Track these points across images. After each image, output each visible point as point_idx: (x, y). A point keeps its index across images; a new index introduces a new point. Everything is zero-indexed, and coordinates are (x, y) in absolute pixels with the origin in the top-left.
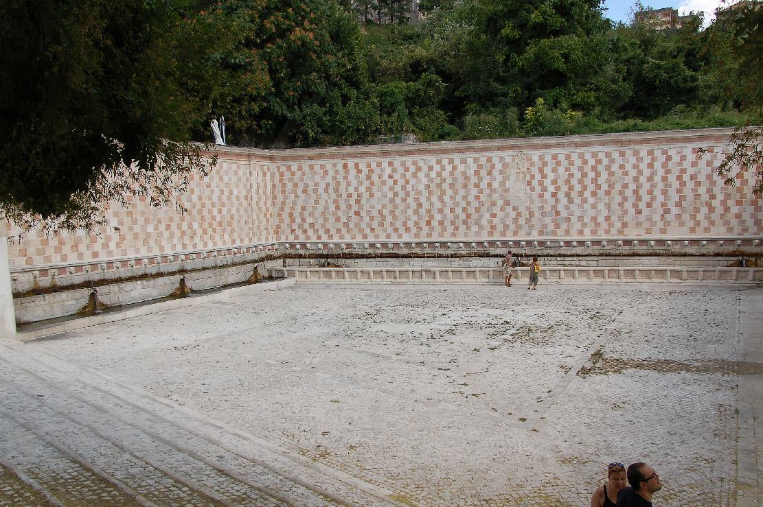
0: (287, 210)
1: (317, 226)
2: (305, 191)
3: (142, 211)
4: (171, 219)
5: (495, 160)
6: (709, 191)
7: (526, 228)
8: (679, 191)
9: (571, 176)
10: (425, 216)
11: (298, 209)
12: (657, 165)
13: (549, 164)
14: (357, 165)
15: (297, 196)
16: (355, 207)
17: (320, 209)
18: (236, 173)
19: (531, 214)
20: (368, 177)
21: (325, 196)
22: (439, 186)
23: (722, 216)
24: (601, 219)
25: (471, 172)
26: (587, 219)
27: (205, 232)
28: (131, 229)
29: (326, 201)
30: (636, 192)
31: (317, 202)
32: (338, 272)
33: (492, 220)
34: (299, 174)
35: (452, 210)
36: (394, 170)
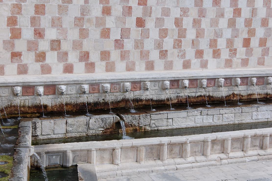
1: (65, 46)
32: (171, 145)
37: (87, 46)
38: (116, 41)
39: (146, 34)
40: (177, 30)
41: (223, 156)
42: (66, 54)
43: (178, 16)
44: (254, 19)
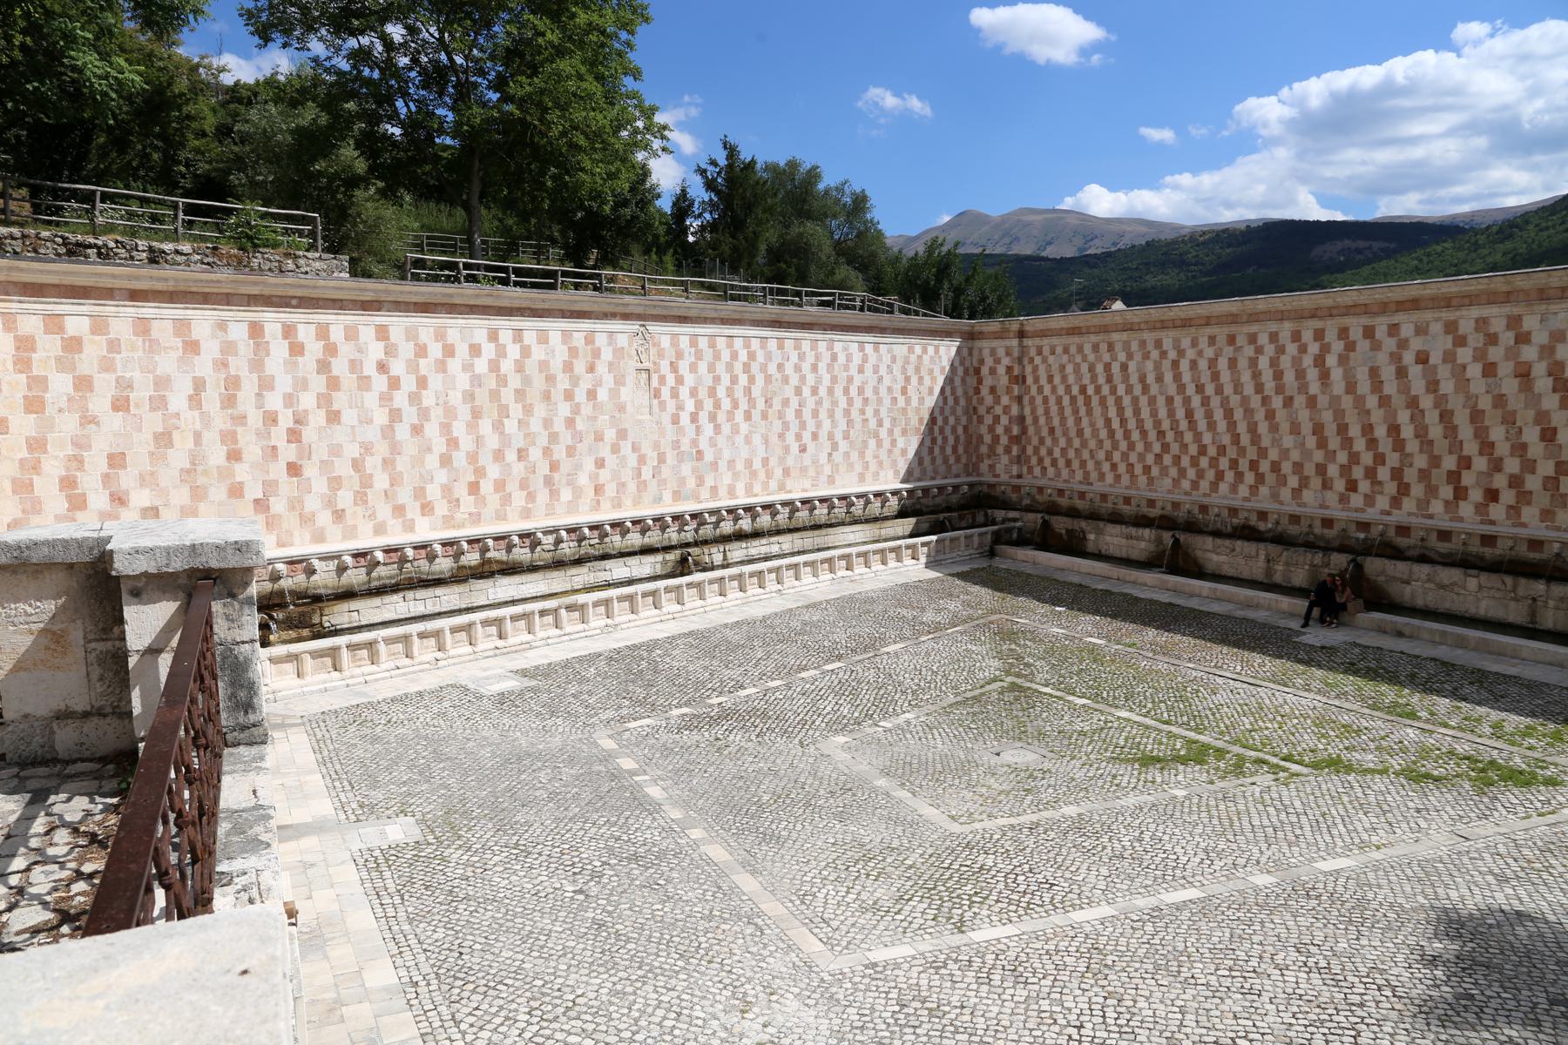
0: (53, 467)
2: (120, 405)
5: (601, 340)
6: (877, 412)
7: (653, 486)
8: (847, 412)
9: (717, 379)
12: (822, 366)
13: (686, 354)
15: (89, 420)
16: (288, 452)
17: (178, 457)
19: (662, 459)
20: (323, 366)
21: (191, 419)
22: (495, 395)
23: (890, 451)
24: (757, 464)
25: (557, 365)
26: (740, 466)
29: (198, 436)
30: (799, 413)
31: (164, 439)
33: (597, 474)
35: (522, 454)
36: (390, 351)
38: (256, 501)
41: (439, 655)
43: (357, 455)
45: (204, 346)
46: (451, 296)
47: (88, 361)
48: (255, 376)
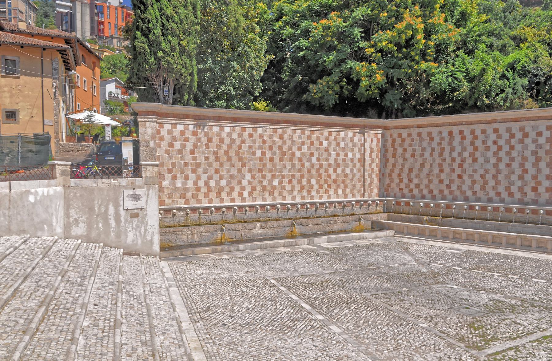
0: (397, 171)
1: (422, 187)
2: (413, 156)
3: (270, 169)
4: (293, 176)
10: (530, 183)
11: (406, 170)
14: (461, 132)
15: (405, 160)
16: (458, 171)
17: (426, 171)
18: (352, 140)
20: (472, 143)
21: (430, 160)
27: (321, 187)
28: (260, 182)
29: (431, 165)
31: (422, 165)
34: (408, 141)
36: (500, 137)
37: (432, 187)
38: (447, 185)
39: (463, 182)
40: (482, 181)
42: (422, 190)
43: (483, 173)
44: (539, 175)
45: (435, 138)
46: (526, 114)
47: (406, 145)
48: (449, 147)
